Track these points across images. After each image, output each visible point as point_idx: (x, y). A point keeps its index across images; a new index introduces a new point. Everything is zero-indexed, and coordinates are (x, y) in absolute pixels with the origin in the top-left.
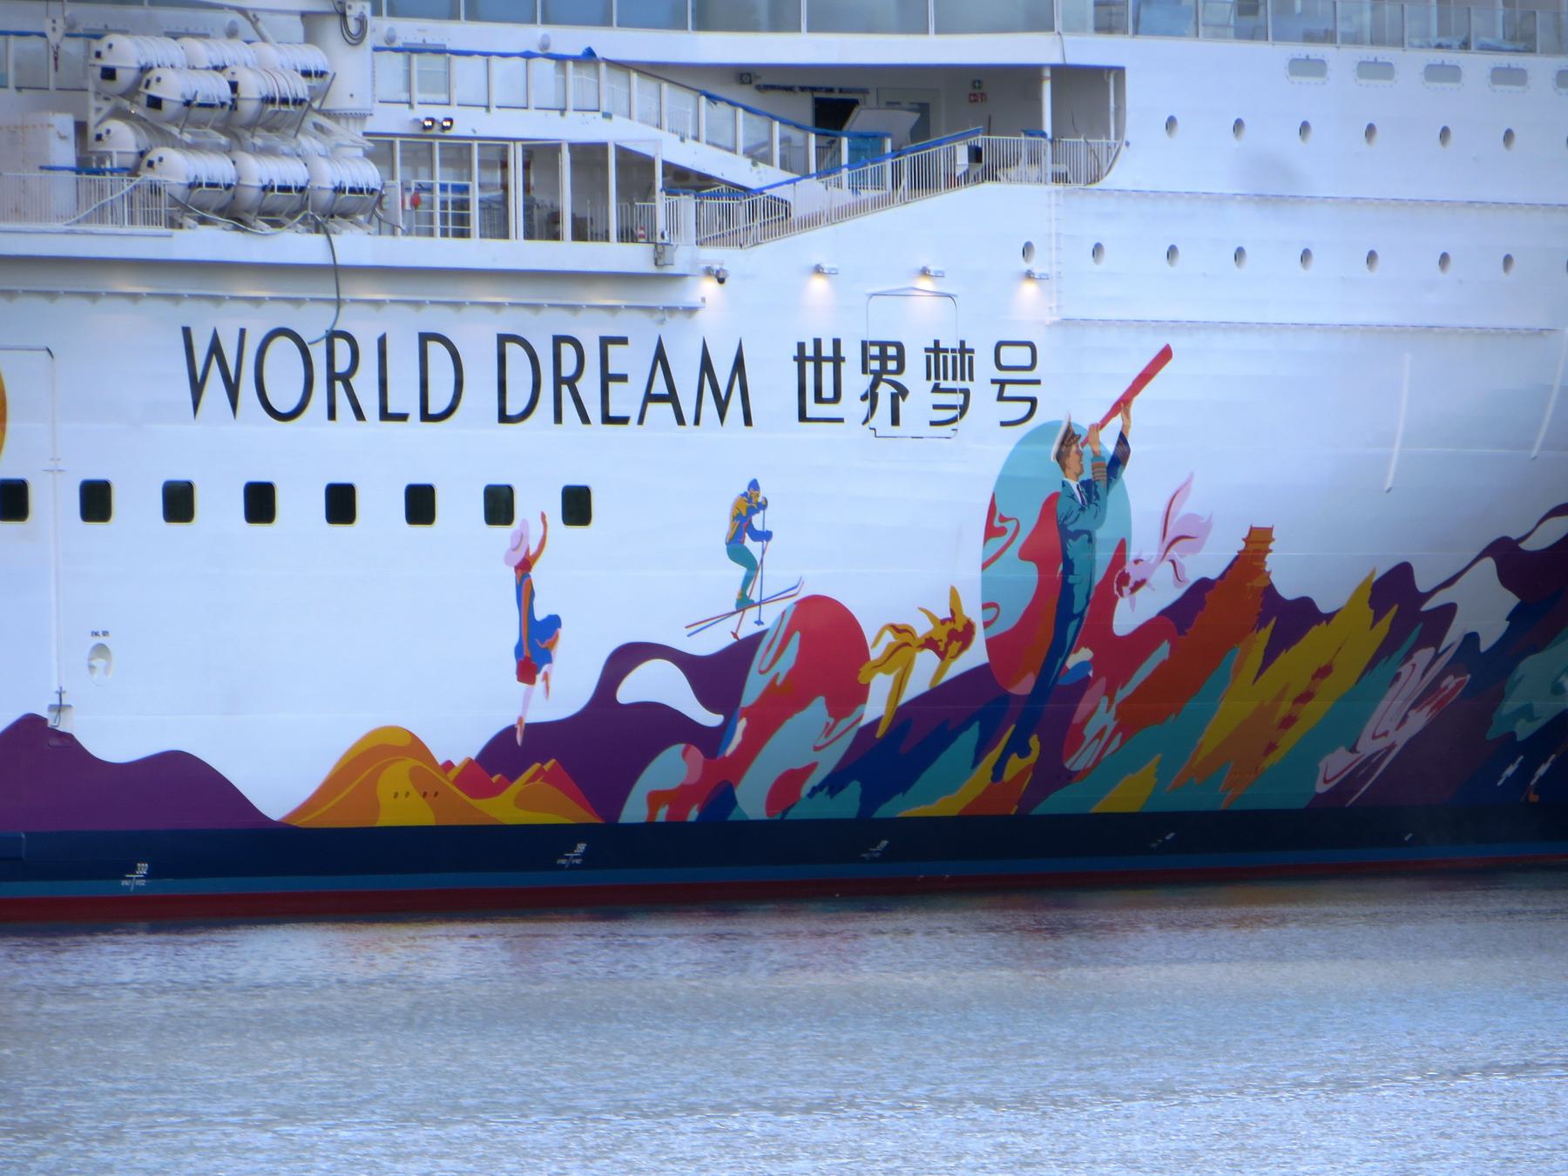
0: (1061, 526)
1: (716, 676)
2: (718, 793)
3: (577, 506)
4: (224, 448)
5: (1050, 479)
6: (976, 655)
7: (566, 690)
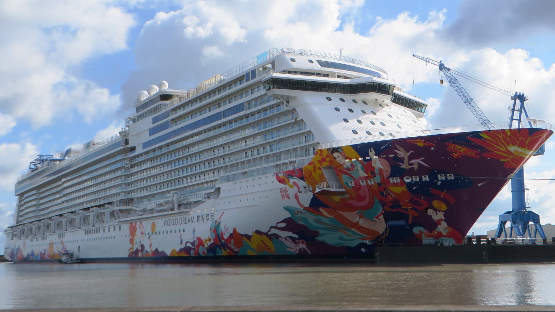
0: (216, 229)
1: (193, 244)
2: (197, 252)
3: (184, 231)
4: (166, 228)
5: (215, 225)
6: (212, 241)
7: (183, 246)
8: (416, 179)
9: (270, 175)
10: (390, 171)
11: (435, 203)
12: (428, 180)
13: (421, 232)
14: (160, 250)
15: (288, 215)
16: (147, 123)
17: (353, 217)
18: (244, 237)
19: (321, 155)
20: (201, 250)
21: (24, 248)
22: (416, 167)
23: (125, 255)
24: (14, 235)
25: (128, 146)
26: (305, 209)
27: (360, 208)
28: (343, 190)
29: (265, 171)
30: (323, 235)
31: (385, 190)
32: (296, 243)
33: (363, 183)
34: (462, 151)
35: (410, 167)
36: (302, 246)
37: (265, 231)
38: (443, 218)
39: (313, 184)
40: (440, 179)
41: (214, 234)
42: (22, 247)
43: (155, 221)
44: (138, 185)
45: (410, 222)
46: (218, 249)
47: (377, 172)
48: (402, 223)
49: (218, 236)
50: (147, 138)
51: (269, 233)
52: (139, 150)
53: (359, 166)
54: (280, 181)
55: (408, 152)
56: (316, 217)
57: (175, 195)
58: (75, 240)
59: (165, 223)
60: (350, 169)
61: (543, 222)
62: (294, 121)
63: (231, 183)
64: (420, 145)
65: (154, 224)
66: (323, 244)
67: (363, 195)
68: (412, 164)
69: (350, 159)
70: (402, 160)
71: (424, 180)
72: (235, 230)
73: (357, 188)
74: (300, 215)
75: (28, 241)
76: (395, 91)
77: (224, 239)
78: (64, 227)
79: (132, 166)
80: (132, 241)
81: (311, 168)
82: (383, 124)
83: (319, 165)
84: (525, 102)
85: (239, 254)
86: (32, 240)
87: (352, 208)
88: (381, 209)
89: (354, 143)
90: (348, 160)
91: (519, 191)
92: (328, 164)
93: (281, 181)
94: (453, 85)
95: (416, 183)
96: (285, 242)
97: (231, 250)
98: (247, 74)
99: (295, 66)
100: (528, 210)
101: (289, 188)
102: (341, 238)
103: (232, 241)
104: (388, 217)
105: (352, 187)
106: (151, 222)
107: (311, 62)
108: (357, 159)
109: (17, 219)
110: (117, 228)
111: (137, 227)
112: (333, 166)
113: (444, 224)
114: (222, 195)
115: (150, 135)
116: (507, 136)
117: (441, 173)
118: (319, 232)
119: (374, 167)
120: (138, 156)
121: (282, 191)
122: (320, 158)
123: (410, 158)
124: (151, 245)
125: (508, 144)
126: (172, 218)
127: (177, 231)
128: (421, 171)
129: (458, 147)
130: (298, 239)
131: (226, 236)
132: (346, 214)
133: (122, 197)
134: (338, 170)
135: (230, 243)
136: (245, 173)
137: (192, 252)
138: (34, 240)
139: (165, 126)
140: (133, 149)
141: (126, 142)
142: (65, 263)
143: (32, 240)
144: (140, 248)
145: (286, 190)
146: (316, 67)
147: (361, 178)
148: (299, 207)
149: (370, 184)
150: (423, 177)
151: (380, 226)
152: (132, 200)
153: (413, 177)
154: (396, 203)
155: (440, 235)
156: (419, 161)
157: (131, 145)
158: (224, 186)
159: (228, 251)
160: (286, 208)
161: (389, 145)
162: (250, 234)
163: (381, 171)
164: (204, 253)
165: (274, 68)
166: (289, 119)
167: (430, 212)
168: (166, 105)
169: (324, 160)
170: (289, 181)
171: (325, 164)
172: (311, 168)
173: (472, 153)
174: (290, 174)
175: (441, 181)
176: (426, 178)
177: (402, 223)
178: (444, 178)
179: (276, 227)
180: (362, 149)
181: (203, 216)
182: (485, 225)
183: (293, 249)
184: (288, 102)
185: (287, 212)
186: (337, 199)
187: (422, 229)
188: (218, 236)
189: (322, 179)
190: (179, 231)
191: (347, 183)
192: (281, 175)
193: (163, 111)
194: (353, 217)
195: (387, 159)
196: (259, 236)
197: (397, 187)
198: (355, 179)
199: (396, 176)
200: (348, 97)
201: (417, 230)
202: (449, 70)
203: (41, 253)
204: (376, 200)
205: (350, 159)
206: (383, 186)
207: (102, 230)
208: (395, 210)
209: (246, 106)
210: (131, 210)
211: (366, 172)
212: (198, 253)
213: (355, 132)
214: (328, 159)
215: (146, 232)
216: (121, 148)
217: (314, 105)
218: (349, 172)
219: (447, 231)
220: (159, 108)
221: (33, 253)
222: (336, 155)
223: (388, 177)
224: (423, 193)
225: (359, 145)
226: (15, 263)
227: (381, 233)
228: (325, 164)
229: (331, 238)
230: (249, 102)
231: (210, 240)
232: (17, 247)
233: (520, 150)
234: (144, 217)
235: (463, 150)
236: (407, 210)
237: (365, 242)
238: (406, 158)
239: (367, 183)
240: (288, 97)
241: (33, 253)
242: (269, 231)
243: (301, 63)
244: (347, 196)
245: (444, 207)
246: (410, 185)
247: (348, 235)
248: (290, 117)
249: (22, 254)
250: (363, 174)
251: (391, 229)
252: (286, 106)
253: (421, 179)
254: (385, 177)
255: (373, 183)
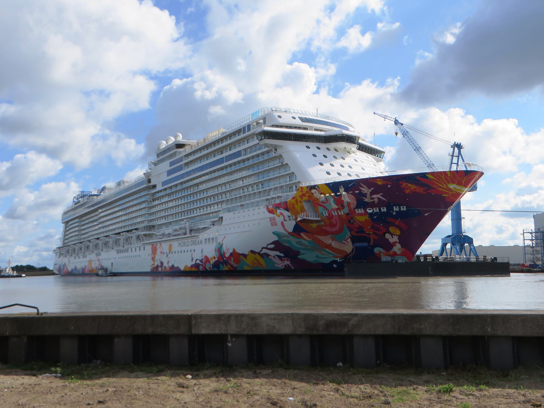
0: (219, 250)
1: (201, 261)
2: (205, 268)
3: (194, 251)
4: (180, 249)
5: (218, 246)
6: (216, 259)
7: (194, 263)
8: (376, 210)
9: (262, 207)
10: (356, 204)
11: (391, 229)
12: (386, 211)
13: (380, 252)
14: (176, 266)
15: (276, 238)
16: (166, 166)
17: (327, 240)
18: (242, 256)
19: (302, 191)
20: (208, 266)
21: (69, 264)
22: (376, 200)
23: (148, 269)
24: (61, 254)
25: (151, 184)
26: (289, 233)
27: (332, 233)
28: (319, 219)
29: (258, 204)
30: (303, 254)
31: (352, 218)
32: (282, 260)
33: (335, 214)
34: (412, 188)
35: (372, 200)
36: (287, 262)
37: (258, 251)
38: (398, 241)
39: (296, 214)
40: (395, 210)
41: (218, 254)
42: (67, 264)
43: (172, 243)
44: (159, 215)
45: (371, 244)
46: (221, 265)
47: (345, 204)
48: (365, 244)
49: (221, 255)
50: (165, 178)
51: (261, 253)
52: (159, 188)
53: (332, 200)
54: (270, 212)
55: (370, 189)
56: (298, 240)
57: (187, 223)
58: (109, 258)
59: (180, 244)
60: (324, 203)
61: (476, 244)
62: (280, 164)
63: (231, 213)
64: (380, 183)
65: (170, 246)
66: (304, 261)
67: (334, 223)
68: (373, 199)
69: (325, 194)
70: (365, 195)
71: (382, 211)
72: (234, 250)
73: (330, 217)
74: (285, 238)
75: (72, 259)
76: (360, 141)
77: (225, 257)
78: (100, 248)
79: (154, 200)
80: (153, 259)
81: (294, 201)
82: (350, 167)
83: (300, 199)
84: (462, 150)
85: (237, 269)
86: (75, 258)
87: (326, 233)
88: (349, 233)
89: (327, 182)
90: (323, 195)
91: (457, 220)
92: (307, 198)
93: (271, 212)
94: (406, 136)
95: (376, 213)
96: (273, 259)
97: (231, 265)
98: (244, 128)
99: (281, 121)
100: (464, 234)
101: (277, 218)
102: (317, 257)
103: (232, 259)
104: (354, 240)
105: (326, 216)
106: (168, 243)
107: (294, 118)
108: (330, 195)
109: (64, 241)
110: (142, 248)
111: (158, 247)
112: (311, 200)
113: (398, 246)
114: (224, 222)
115: (168, 176)
116: (448, 177)
117: (396, 205)
118: (300, 252)
119: (343, 201)
120: (158, 192)
121: (272, 220)
122: (301, 194)
123: (372, 193)
124: (168, 262)
125: (449, 182)
126: (185, 241)
127: (189, 251)
128: (380, 204)
129: (410, 185)
130: (284, 257)
131: (227, 255)
132: (321, 238)
133: (146, 224)
134: (315, 203)
135: (231, 260)
136: (242, 205)
137: (201, 267)
138: (77, 258)
139: (180, 168)
140: (154, 186)
141: (149, 181)
142: (101, 276)
143: (75, 258)
144: (160, 265)
145: (274, 219)
146: (298, 122)
147: (333, 210)
148: (284, 232)
149: (340, 214)
150: (382, 208)
151: (348, 247)
152: (154, 226)
153: (374, 209)
154: (361, 229)
155: (395, 254)
156: (379, 196)
157: (153, 183)
158: (226, 216)
159: (229, 266)
160: (274, 233)
161: (354, 184)
162: (246, 253)
163: (348, 203)
164: (210, 268)
165: (265, 123)
166: (277, 163)
167: (388, 236)
168: (180, 152)
169: (304, 195)
170: (276, 212)
171: (305, 198)
172: (294, 201)
173: (420, 190)
174: (278, 206)
175: (396, 211)
176: (384, 210)
177: (365, 244)
178: (398, 210)
179: (266, 248)
180: (334, 187)
181: (209, 239)
182: (430, 246)
183: (280, 265)
184: (276, 150)
185: (275, 236)
186: (314, 225)
187: (381, 250)
188: (221, 255)
189: (303, 210)
190: (191, 251)
191: (322, 213)
192: (270, 207)
193: (178, 157)
194: (327, 240)
195: (354, 194)
196: (253, 255)
197: (361, 216)
198: (328, 210)
199: (360, 208)
200: (323, 146)
201: (377, 250)
202: (402, 124)
203: (82, 268)
204: (345, 227)
205: (325, 194)
206: (350, 216)
207: (130, 250)
208: (360, 234)
209: (243, 152)
210: (153, 234)
211: (337, 205)
212: (205, 268)
213: (328, 173)
214: (307, 195)
215: (165, 252)
216: (145, 185)
217: (296, 151)
218: (324, 205)
219: (401, 251)
220: (174, 154)
221: (76, 269)
222: (313, 191)
223: (354, 209)
224: (382, 221)
225: (331, 183)
226: (62, 276)
227: (349, 253)
228: (305, 198)
229: (309, 256)
230: (245, 150)
231: (214, 258)
232: (63, 264)
233: (458, 187)
234: (163, 240)
235: (413, 187)
236: (369, 234)
237: (336, 259)
238: (368, 193)
239: (338, 213)
240: (276, 146)
241: (76, 269)
242: (261, 251)
243: (286, 119)
244: (322, 223)
245: (398, 232)
246: (371, 215)
247: (323, 254)
248: (278, 161)
249: (67, 269)
250: (335, 206)
251: (357, 250)
252: (275, 153)
253: (380, 210)
254: (352, 208)
255: (343, 214)
